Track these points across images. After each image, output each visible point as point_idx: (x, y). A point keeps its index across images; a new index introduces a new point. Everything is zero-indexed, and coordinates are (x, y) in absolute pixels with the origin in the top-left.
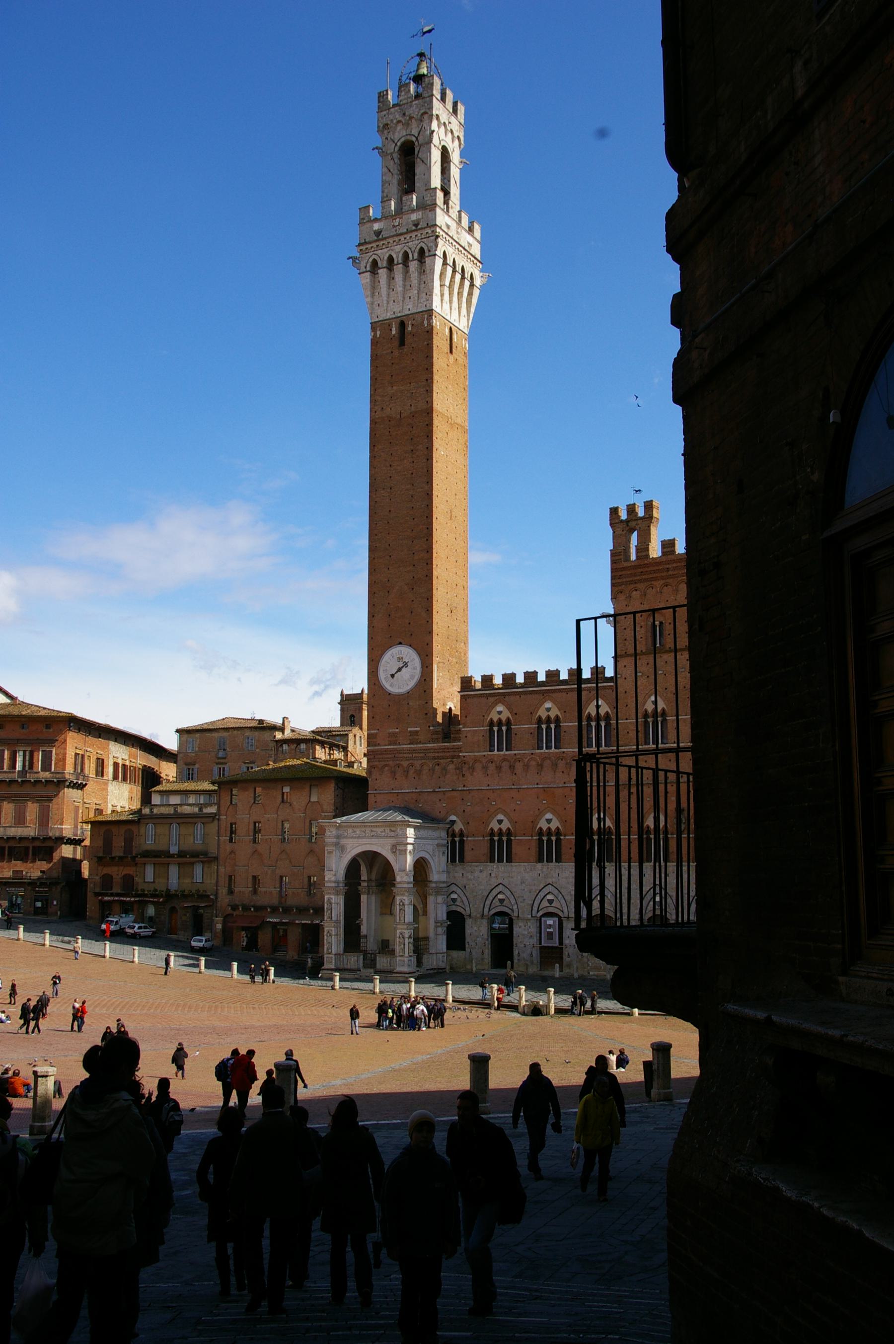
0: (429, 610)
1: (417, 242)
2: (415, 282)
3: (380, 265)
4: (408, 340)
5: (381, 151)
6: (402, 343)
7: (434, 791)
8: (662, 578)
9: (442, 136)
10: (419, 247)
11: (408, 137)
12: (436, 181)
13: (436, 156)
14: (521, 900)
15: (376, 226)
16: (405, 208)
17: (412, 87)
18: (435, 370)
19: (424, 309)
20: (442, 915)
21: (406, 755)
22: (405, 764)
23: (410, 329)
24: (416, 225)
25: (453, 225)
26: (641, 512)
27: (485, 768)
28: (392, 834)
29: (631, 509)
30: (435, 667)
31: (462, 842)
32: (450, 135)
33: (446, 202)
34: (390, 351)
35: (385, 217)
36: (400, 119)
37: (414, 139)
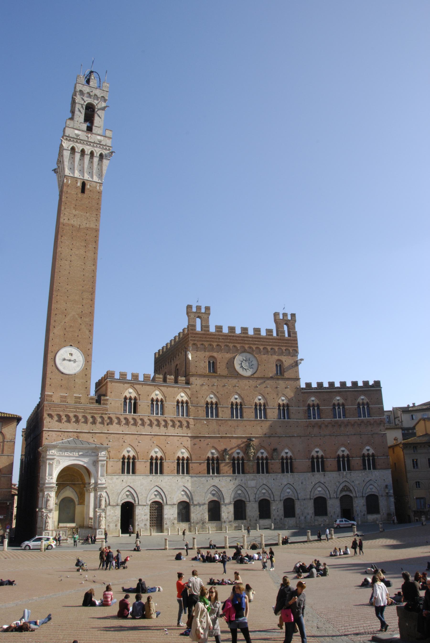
0: (91, 331)
1: (99, 149)
3: (77, 150)
4: (86, 192)
8: (216, 342)
11: (92, 102)
14: (141, 494)
21: (72, 410)
23: (88, 187)
24: (100, 142)
26: (203, 310)
28: (93, 454)
29: (199, 308)
34: (76, 193)
37: (95, 105)
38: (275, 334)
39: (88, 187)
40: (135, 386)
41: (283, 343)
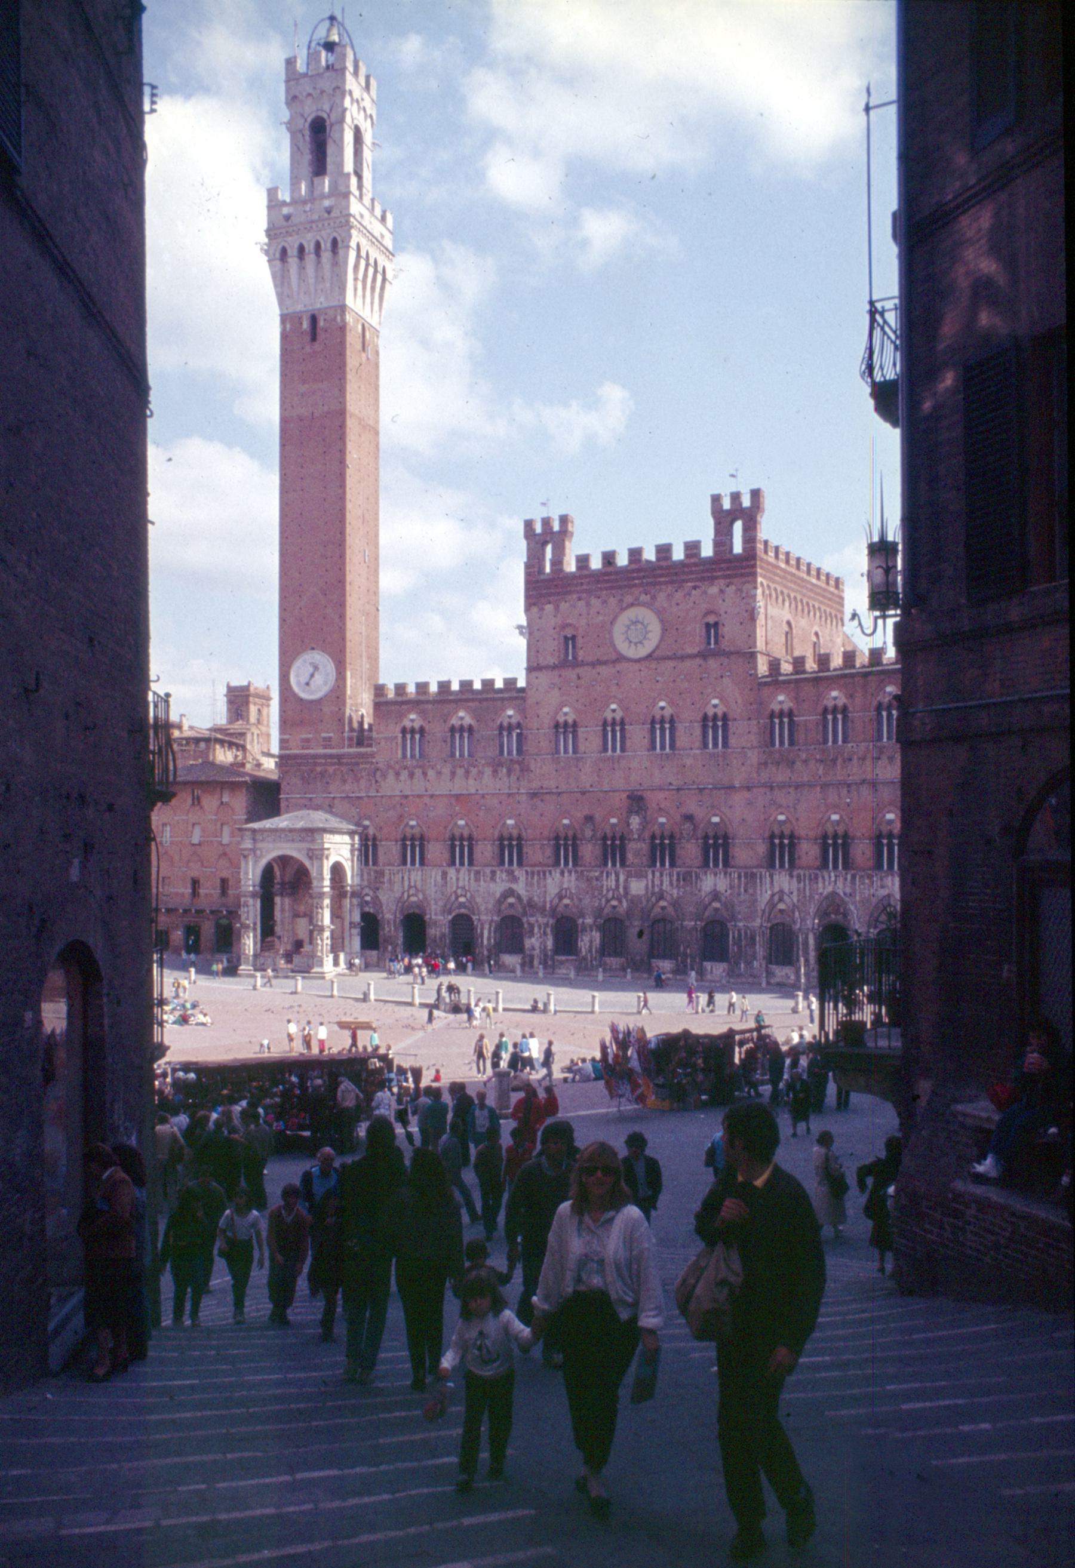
0: (342, 617)
1: (329, 231)
2: (327, 273)
3: (289, 252)
4: (321, 336)
5: (291, 127)
6: (314, 338)
7: (347, 797)
9: (355, 114)
10: (331, 237)
11: (320, 114)
12: (349, 166)
13: (349, 137)
15: (285, 211)
16: (317, 193)
17: (323, 54)
18: (348, 369)
19: (336, 303)
20: (357, 918)
22: (319, 769)
25: (366, 213)
26: (556, 527)
27: (398, 774)
29: (546, 522)
30: (348, 674)
31: (375, 846)
32: (362, 112)
33: (360, 187)
35: (294, 202)
36: (311, 91)
37: (325, 116)
38: (707, 551)
39: (321, 323)
40: (422, 707)
41: (721, 569)
